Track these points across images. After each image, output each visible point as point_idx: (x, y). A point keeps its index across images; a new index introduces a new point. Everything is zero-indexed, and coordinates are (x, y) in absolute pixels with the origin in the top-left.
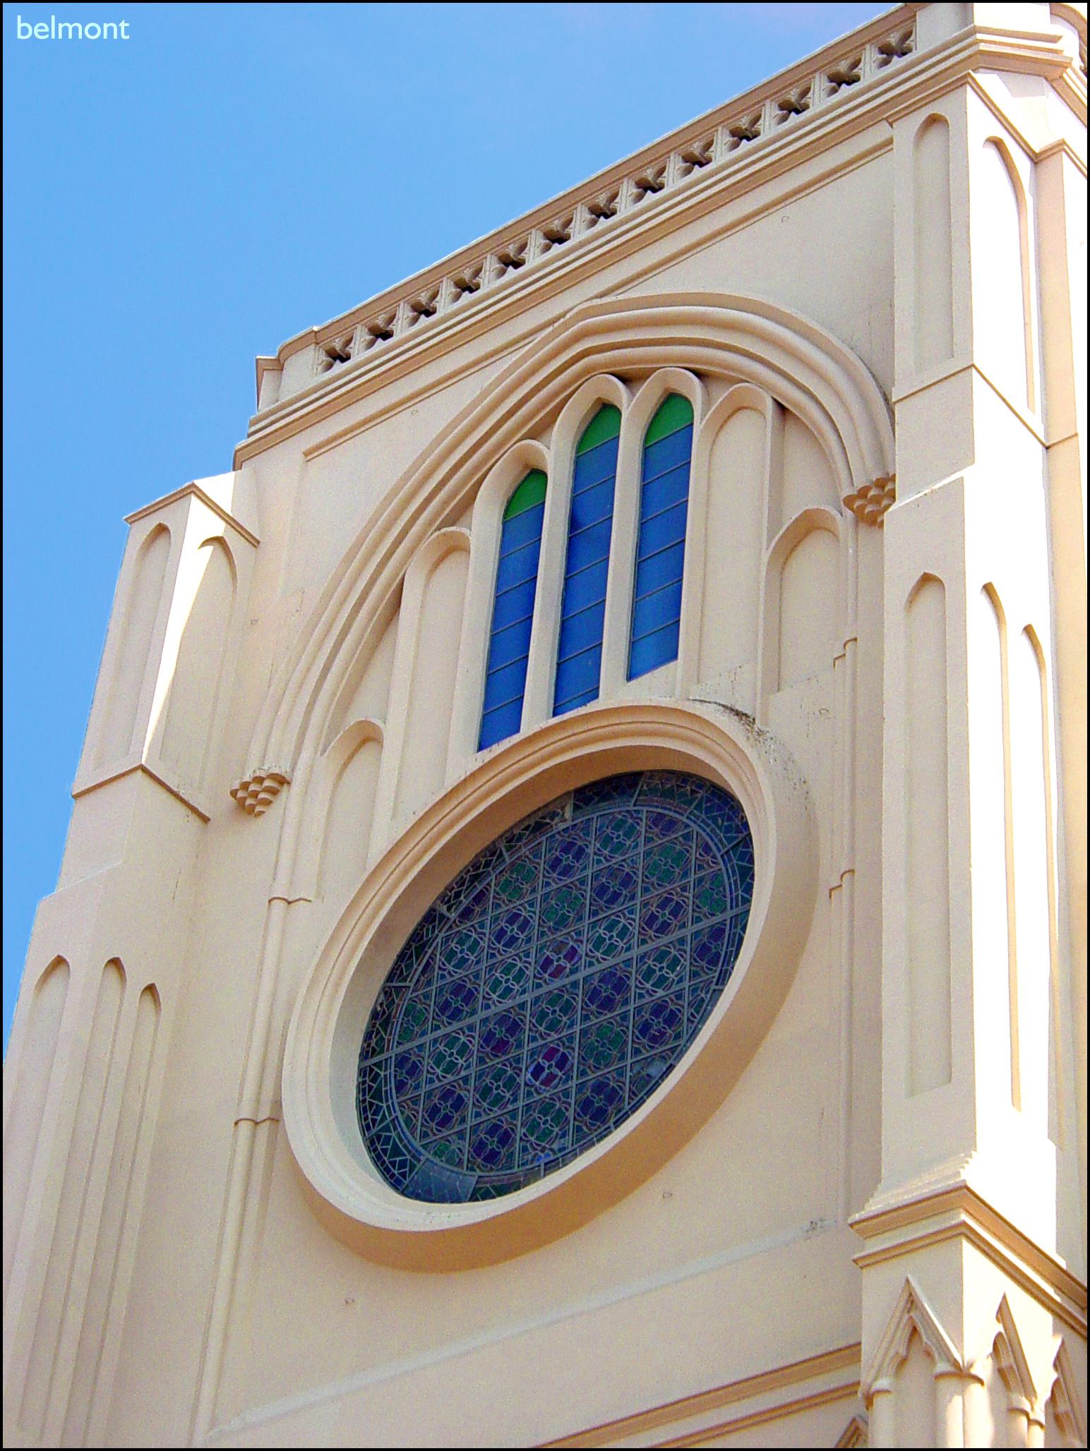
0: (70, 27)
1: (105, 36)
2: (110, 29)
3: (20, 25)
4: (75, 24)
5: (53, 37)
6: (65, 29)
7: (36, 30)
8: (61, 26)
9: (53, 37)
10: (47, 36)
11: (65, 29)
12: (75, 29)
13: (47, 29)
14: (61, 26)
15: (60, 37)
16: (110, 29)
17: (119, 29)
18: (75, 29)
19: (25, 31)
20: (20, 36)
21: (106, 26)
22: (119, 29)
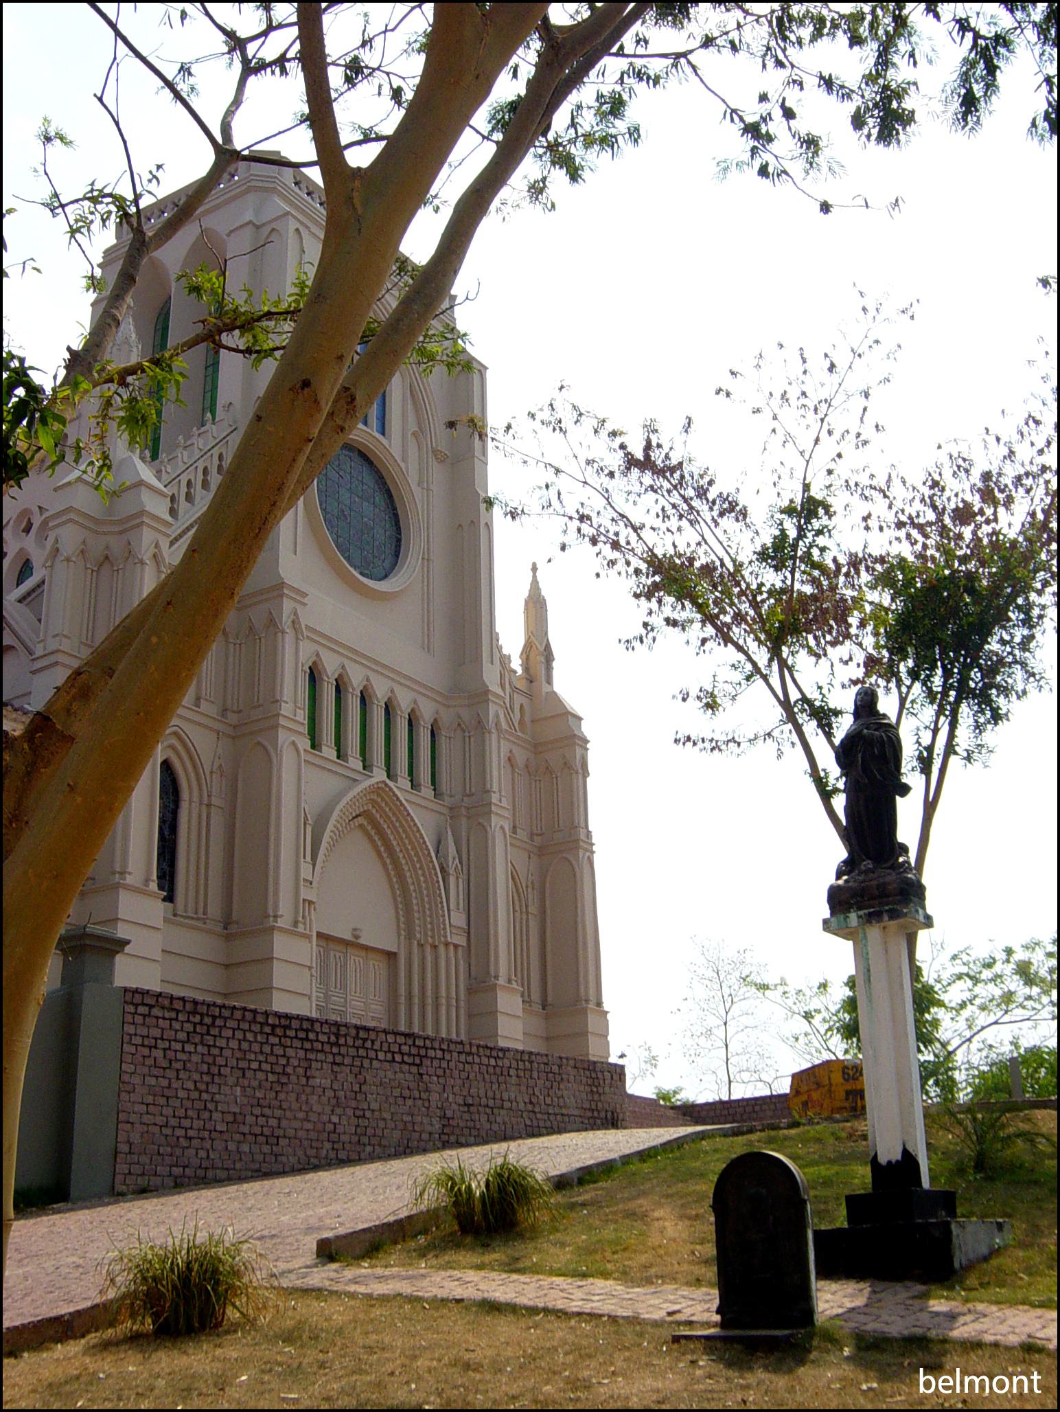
0: (977, 1380)
1: (1015, 1391)
2: (1020, 1382)
3: (922, 1379)
4: (981, 1377)
5: (958, 1391)
6: (971, 1383)
7: (940, 1384)
8: (967, 1379)
9: (958, 1391)
10: (950, 1391)
11: (971, 1383)
12: (982, 1383)
13: (951, 1383)
14: (967, 1379)
15: (966, 1391)
16: (1020, 1382)
17: (1031, 1381)
18: (982, 1383)
19: (927, 1385)
20: (922, 1389)
21: (1015, 1379)
22: (1031, 1381)
